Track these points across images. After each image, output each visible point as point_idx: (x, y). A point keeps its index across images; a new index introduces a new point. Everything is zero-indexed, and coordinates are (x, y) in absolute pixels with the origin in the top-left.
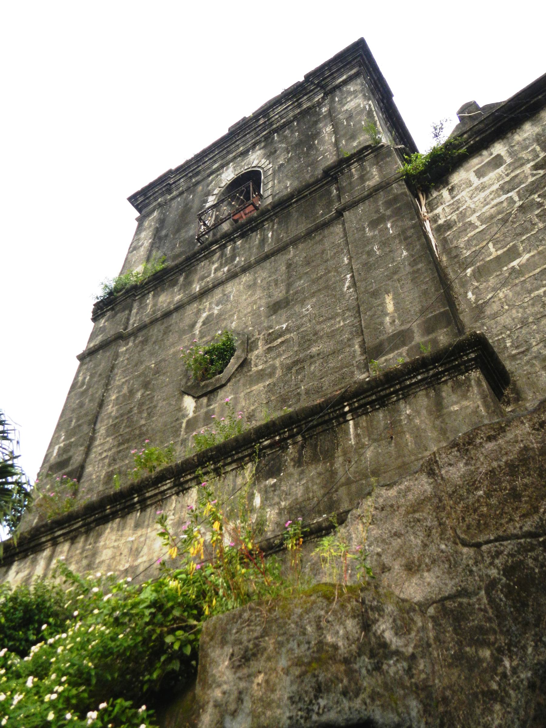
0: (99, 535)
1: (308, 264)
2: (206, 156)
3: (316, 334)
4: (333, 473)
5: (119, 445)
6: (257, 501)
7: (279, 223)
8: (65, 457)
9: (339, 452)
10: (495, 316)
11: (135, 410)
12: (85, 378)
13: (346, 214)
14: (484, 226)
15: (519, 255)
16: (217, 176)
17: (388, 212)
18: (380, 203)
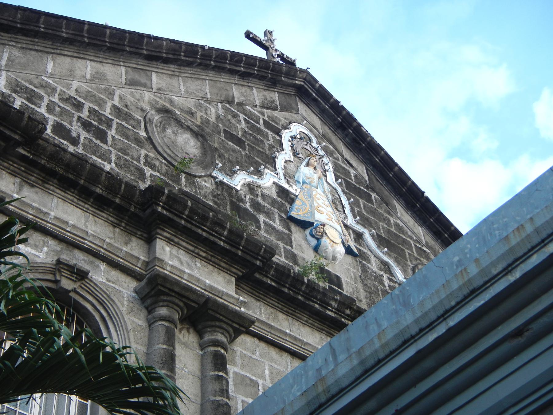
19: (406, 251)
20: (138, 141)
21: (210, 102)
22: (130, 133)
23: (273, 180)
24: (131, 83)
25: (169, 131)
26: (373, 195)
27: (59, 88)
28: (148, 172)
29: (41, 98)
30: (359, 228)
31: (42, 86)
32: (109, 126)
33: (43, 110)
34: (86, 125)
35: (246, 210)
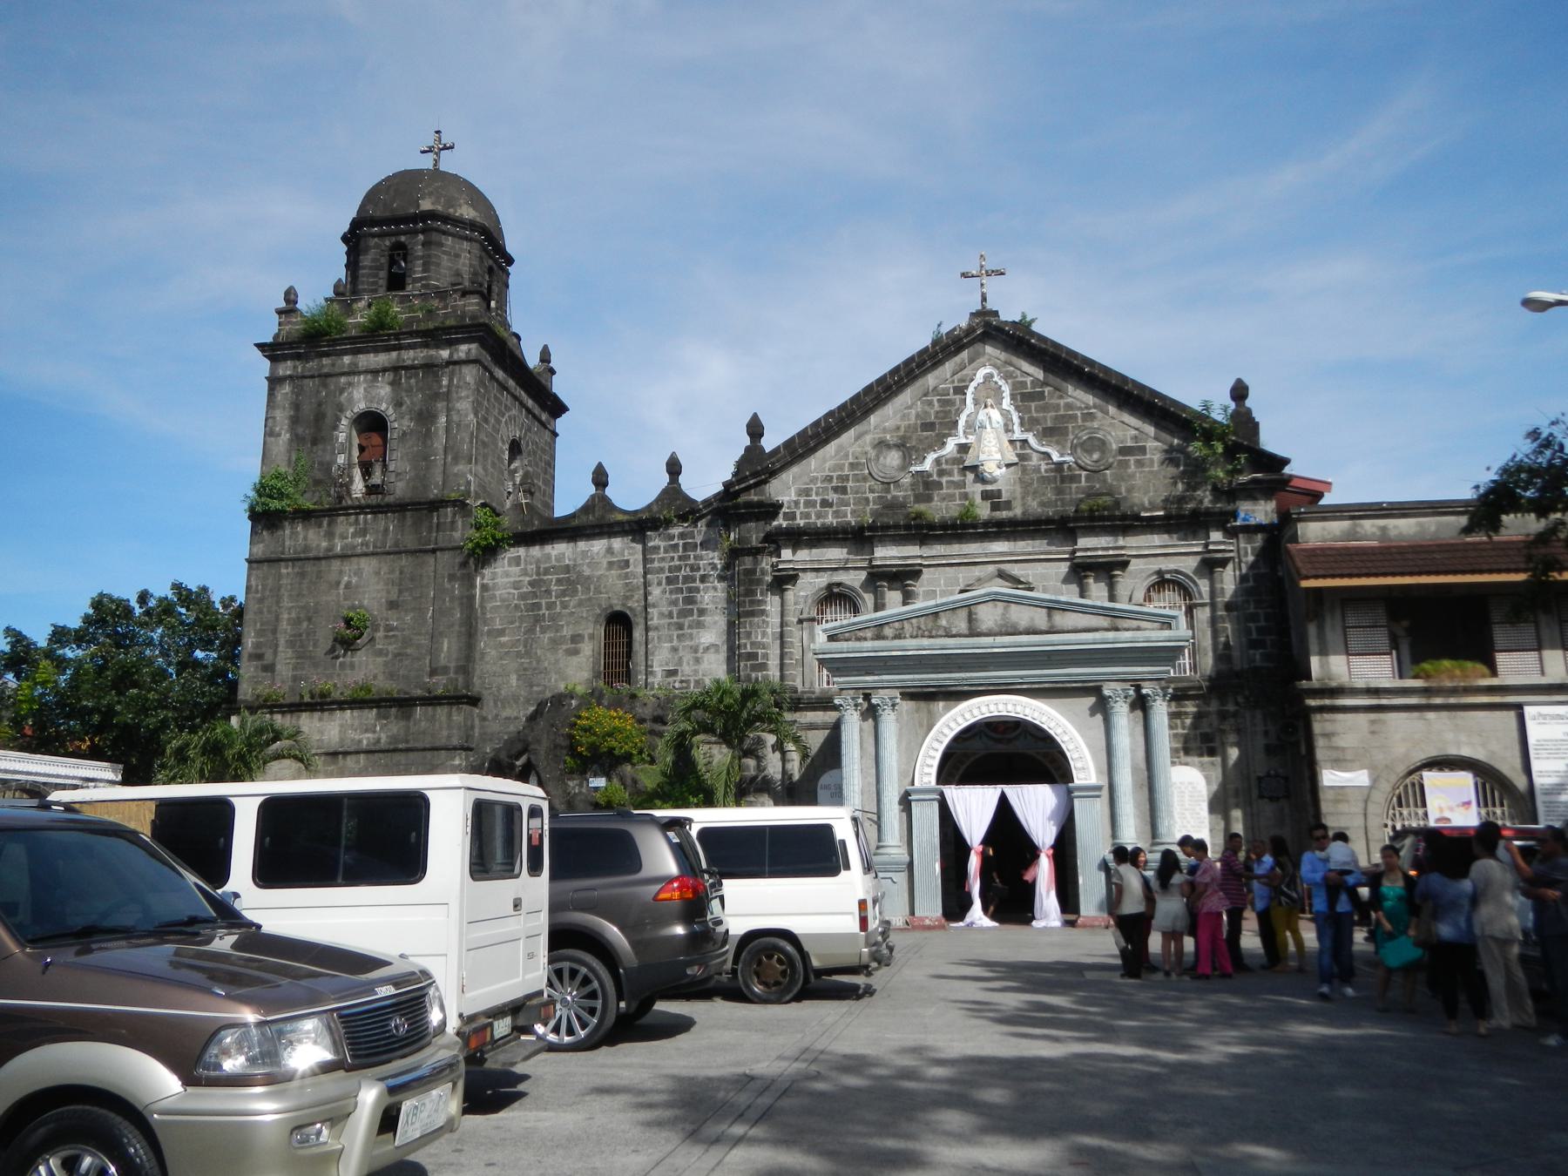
0: (299, 717)
1: (412, 579)
2: (340, 345)
3: (411, 640)
4: (408, 728)
5: (297, 658)
6: (378, 728)
7: (399, 520)
8: (259, 651)
9: (412, 719)
10: (487, 663)
11: (304, 637)
12: (257, 586)
13: (438, 553)
14: (498, 604)
15: (504, 636)
16: (350, 384)
17: (458, 575)
18: (457, 560)
19: (1070, 426)
20: (865, 479)
21: (910, 407)
22: (860, 477)
23: (953, 445)
24: (858, 438)
25: (882, 458)
26: (1047, 390)
27: (819, 475)
28: (871, 496)
29: (812, 489)
30: (1024, 436)
31: (811, 481)
32: (848, 480)
33: (814, 497)
34: (836, 490)
35: (934, 481)
